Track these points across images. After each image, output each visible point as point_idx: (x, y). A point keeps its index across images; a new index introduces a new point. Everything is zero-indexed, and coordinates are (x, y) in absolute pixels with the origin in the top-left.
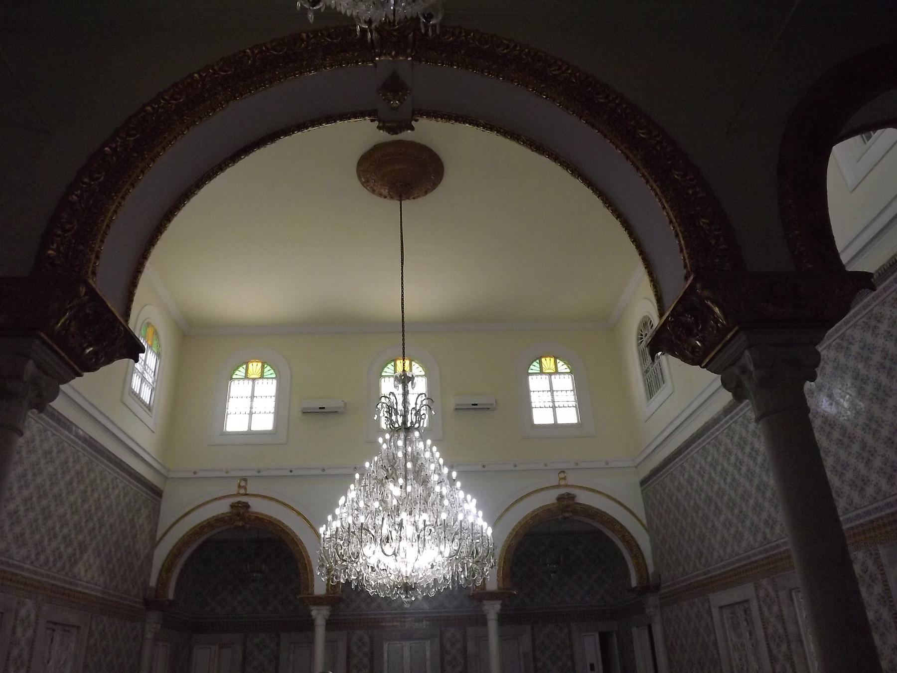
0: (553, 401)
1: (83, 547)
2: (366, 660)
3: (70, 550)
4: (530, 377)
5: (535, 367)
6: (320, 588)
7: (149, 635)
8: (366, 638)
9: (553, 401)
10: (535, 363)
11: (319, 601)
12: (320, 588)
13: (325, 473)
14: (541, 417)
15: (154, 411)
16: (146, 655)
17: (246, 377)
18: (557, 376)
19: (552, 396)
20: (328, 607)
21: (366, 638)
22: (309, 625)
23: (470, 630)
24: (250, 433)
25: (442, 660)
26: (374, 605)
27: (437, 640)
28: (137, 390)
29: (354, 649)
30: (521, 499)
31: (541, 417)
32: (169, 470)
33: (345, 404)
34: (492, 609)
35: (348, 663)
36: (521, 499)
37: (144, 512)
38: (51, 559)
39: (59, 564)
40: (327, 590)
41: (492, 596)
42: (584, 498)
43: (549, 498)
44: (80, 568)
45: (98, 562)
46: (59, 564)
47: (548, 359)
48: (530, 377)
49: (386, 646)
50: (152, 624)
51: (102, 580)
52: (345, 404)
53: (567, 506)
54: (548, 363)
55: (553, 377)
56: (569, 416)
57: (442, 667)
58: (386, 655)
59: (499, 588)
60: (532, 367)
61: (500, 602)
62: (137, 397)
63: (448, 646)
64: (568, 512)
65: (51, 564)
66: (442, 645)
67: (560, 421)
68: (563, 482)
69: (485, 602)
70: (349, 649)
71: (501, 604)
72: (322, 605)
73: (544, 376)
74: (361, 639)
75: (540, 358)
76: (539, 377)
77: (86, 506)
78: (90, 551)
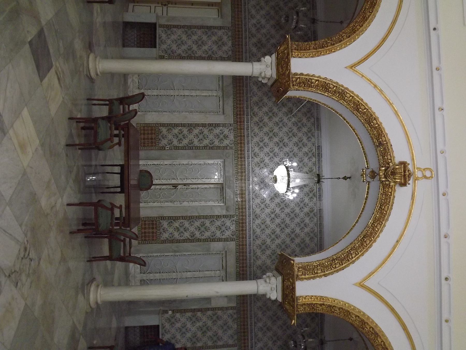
2: (206, 142)
6: (300, 65)
8: (226, 142)
11: (283, 64)
12: (300, 65)
20: (275, 76)
21: (226, 142)
23: (232, 245)
25: (206, 217)
26: (257, 150)
27: (224, 212)
29: (217, 131)
30: (405, 328)
34: (269, 287)
35: (204, 125)
36: (405, 328)
40: (296, 74)
41: (288, 291)
49: (219, 161)
57: (199, 217)
58: (211, 162)
59: (298, 298)
61: (280, 299)
63: (218, 223)
66: (218, 217)
69: (280, 278)
70: (217, 125)
71: (276, 300)
72: (278, 70)
74: (226, 137)
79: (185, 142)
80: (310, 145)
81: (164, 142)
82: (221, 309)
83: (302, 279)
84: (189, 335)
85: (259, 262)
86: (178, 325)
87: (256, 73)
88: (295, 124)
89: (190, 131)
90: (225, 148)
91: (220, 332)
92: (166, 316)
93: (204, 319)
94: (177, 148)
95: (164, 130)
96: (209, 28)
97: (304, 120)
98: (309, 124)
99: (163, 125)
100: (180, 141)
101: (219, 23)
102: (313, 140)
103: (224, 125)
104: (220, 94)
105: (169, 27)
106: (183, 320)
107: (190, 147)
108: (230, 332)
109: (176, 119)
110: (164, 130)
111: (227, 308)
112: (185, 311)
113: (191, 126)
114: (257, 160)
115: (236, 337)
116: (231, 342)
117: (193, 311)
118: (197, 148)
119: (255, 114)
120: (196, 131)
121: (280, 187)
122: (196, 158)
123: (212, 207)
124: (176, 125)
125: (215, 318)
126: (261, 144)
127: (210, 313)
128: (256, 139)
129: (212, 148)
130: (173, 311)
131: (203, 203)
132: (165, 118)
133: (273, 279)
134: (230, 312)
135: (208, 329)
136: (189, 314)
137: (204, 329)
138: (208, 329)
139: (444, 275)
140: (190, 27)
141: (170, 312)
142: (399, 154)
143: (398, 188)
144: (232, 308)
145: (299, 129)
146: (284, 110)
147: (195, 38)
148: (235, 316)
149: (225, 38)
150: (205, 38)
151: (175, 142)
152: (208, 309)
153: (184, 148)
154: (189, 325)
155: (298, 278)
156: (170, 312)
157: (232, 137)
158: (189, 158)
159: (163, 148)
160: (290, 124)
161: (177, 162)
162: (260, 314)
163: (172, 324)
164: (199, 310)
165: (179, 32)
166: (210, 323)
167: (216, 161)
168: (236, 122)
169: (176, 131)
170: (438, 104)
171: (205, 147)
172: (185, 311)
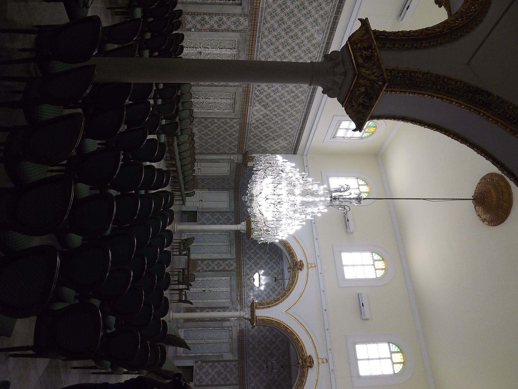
0: (373, 359)
1: (265, 106)
2: (221, 268)
3: (264, 98)
4: (387, 345)
5: (394, 348)
7: (232, 157)
8: (232, 268)
9: (373, 359)
10: (397, 348)
13: (320, 274)
14: (362, 350)
15: (333, 140)
16: (225, 157)
17: (359, 185)
18: (391, 363)
19: (377, 359)
21: (232, 268)
22: (237, 222)
24: (342, 266)
26: (248, 271)
28: (341, 127)
29: (227, 262)
31: (362, 350)
32: (306, 155)
33: (352, 233)
35: (220, 260)
37: (284, 143)
38: (260, 88)
39: (258, 93)
42: (311, 374)
43: (309, 350)
44: (258, 106)
45: (261, 117)
46: (258, 93)
47: (402, 357)
48: (386, 345)
50: (237, 158)
51: (254, 121)
52: (352, 233)
53: (306, 362)
54: (399, 357)
55: (390, 360)
56: (365, 369)
58: (224, 278)
59: (256, 317)
60: (394, 346)
62: (337, 128)
64: (302, 362)
65: (258, 88)
67: (359, 363)
68: (320, 361)
70: (228, 259)
73: (389, 353)
74: (232, 265)
75: (401, 352)
76: (388, 350)
77: (283, 104)
78: (265, 111)
79: (210, 268)
80: (277, 269)
81: (199, 268)
82: (228, 361)
83: (258, 308)
84: (210, 377)
85: (251, 334)
86: (204, 370)
87: (239, 229)
88: (269, 258)
89: (213, 263)
90: (231, 271)
91: (228, 376)
92: (198, 364)
93: (219, 367)
94: (206, 271)
95: (199, 262)
96: (223, 212)
97: (274, 256)
98: (276, 258)
99: (199, 260)
100: (208, 263)
101: (228, 210)
102: (279, 266)
103: (231, 259)
104: (228, 244)
105: (203, 213)
106: (207, 367)
107: (213, 270)
108: (234, 376)
109: (206, 256)
110: (199, 262)
111: (232, 361)
112: (209, 362)
113: (213, 260)
114: (248, 277)
115: (238, 379)
116: (235, 382)
117: (212, 362)
118: (217, 271)
119: (247, 253)
120: (216, 263)
121: (256, 283)
122: (216, 276)
123: (224, 302)
124: (206, 260)
125: (225, 366)
126: (251, 269)
127: (222, 363)
128: (247, 266)
129: (224, 271)
130: (201, 362)
131: (219, 301)
132: (200, 257)
133: (246, 310)
134: (235, 363)
135: (221, 373)
136: (210, 364)
137: (219, 373)
138: (221, 373)
139: (324, 308)
140: (213, 212)
141: (200, 362)
142: (299, 257)
143: (299, 271)
144: (235, 361)
145: (271, 260)
146: (262, 251)
147: (216, 217)
148: (237, 366)
149: (231, 217)
150: (221, 217)
151: (205, 268)
152: (221, 361)
153: (210, 271)
154: (210, 370)
155: (257, 308)
156: (200, 362)
157: (235, 265)
158: (212, 276)
159: (199, 271)
160: (266, 258)
161: (205, 279)
162: (252, 365)
163: (200, 370)
164: (216, 361)
165: (208, 215)
166: (222, 370)
167: (226, 278)
168: (237, 258)
169: (206, 262)
170: (315, 237)
171: (220, 271)
172: (209, 362)
